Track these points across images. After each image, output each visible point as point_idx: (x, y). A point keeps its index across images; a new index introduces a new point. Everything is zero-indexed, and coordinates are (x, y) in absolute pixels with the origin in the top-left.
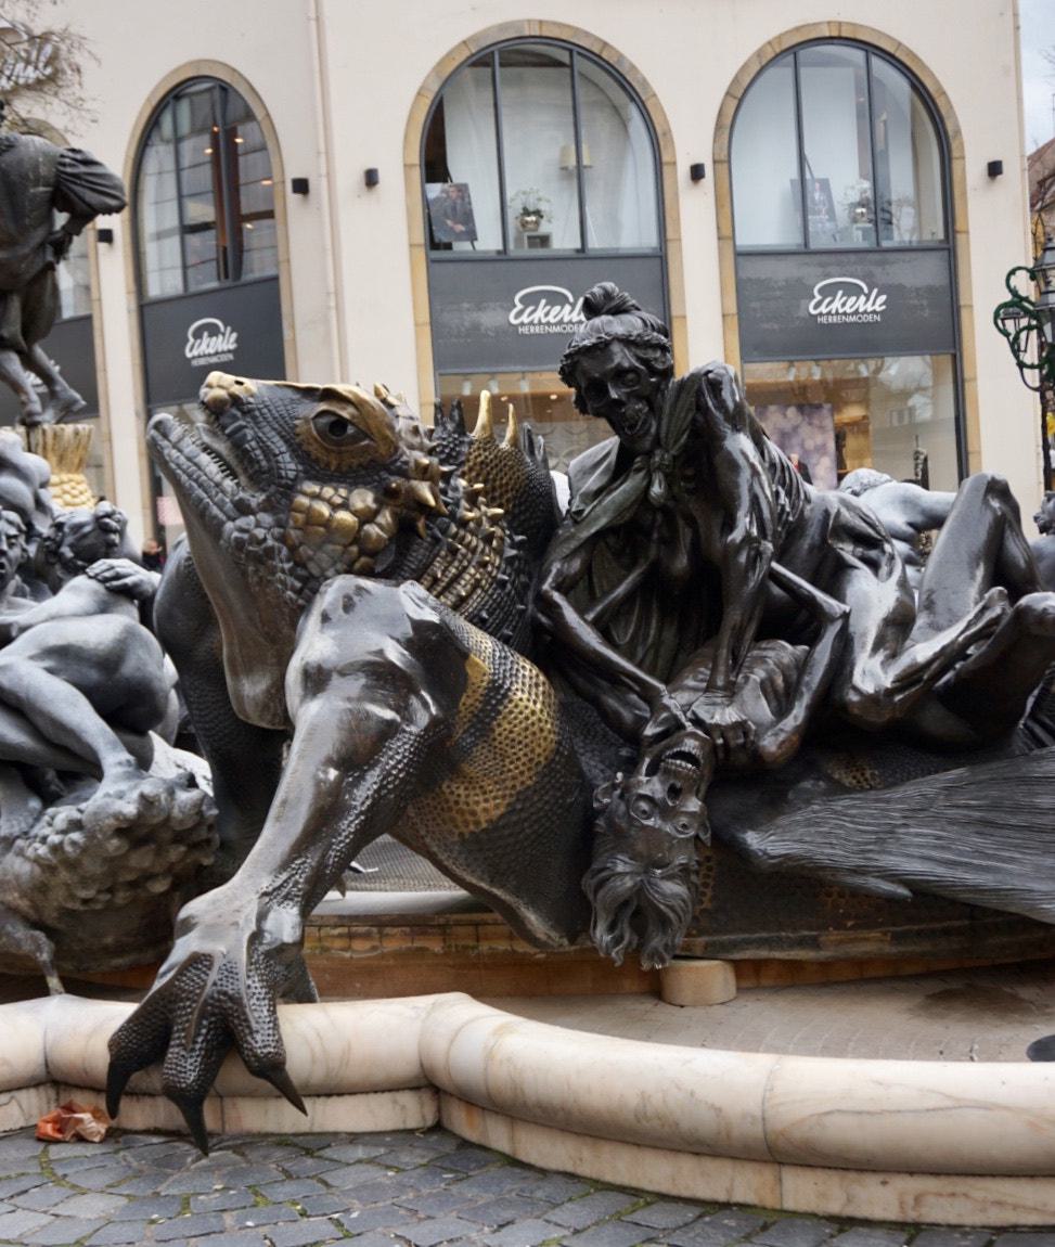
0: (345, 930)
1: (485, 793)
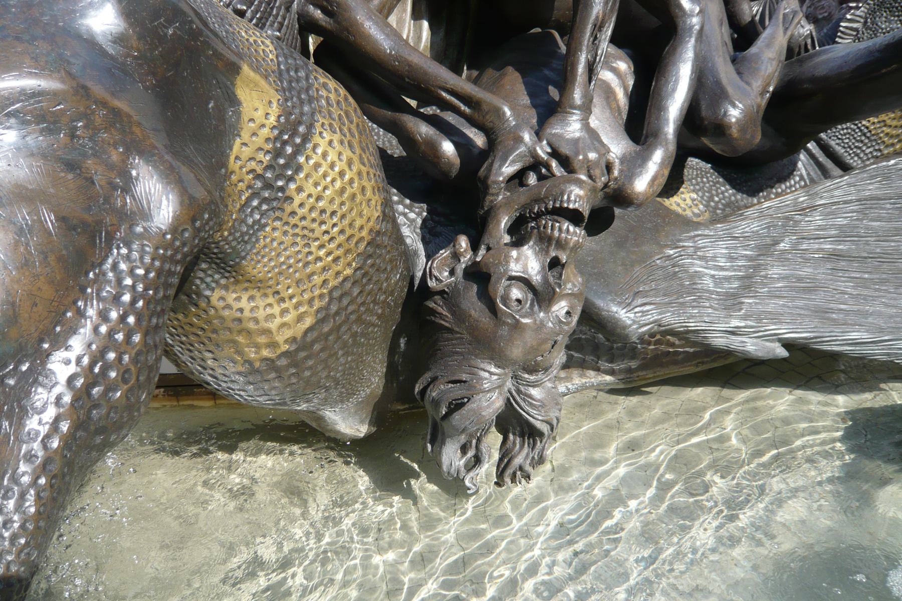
1: (283, 300)
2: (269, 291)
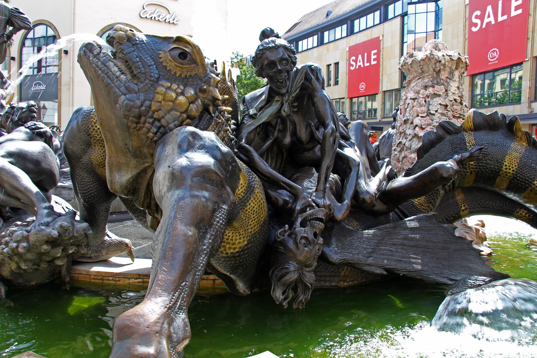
0: (141, 280)
2: (238, 232)
